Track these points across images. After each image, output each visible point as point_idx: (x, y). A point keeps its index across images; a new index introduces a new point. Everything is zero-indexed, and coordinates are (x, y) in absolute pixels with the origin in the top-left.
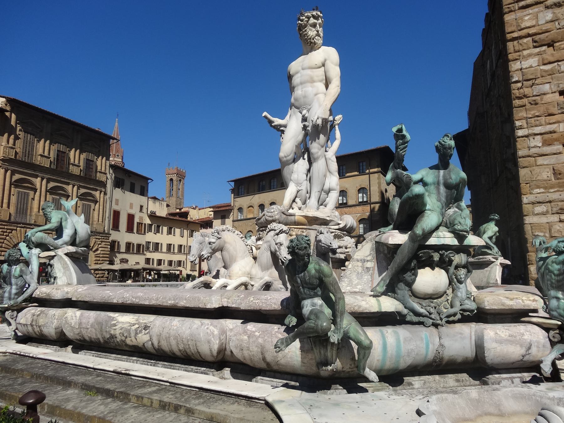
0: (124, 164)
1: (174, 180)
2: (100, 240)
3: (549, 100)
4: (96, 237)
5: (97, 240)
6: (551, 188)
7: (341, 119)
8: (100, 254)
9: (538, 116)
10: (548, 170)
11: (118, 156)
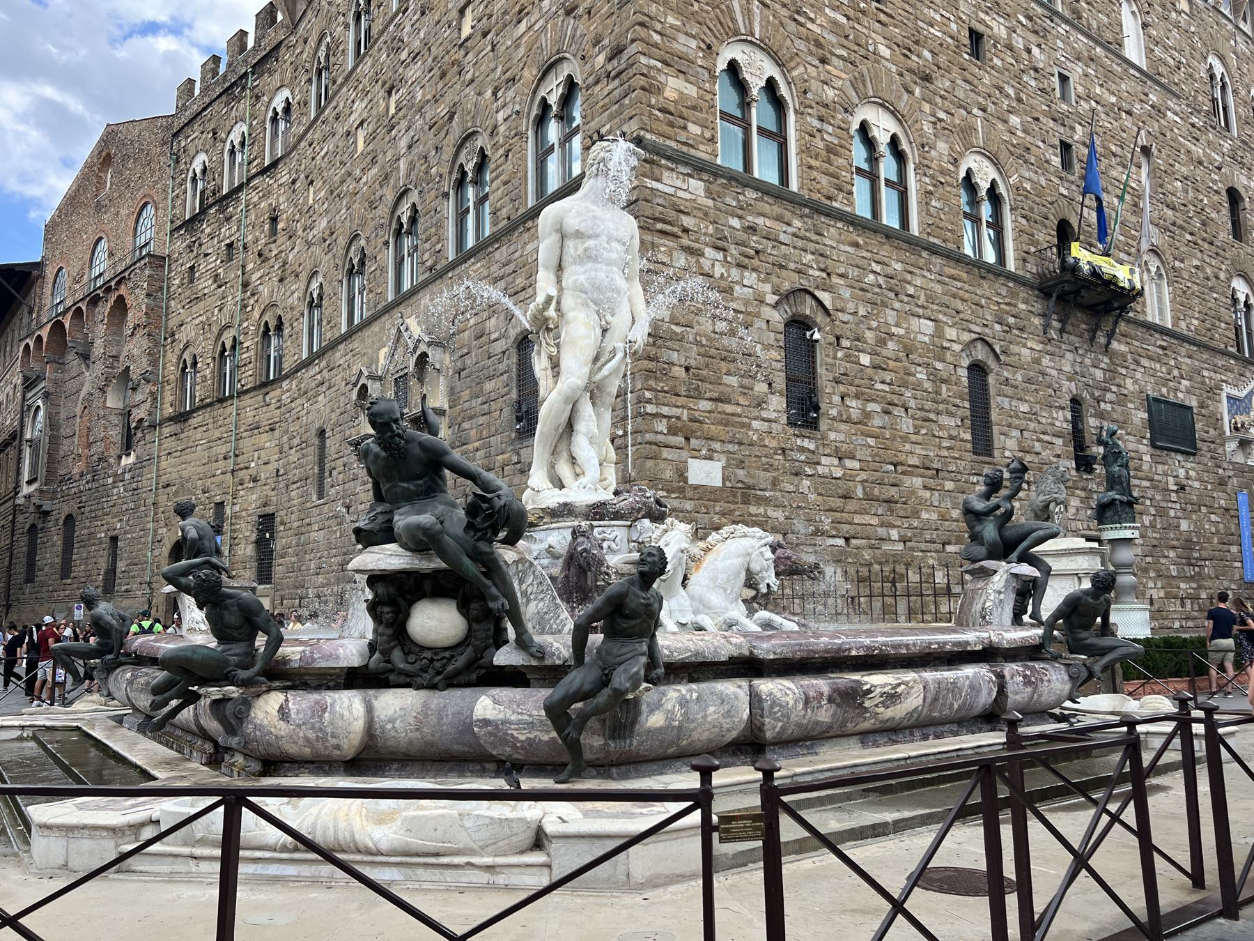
3: (677, 375)
6: (673, 492)
9: (666, 392)
10: (671, 467)
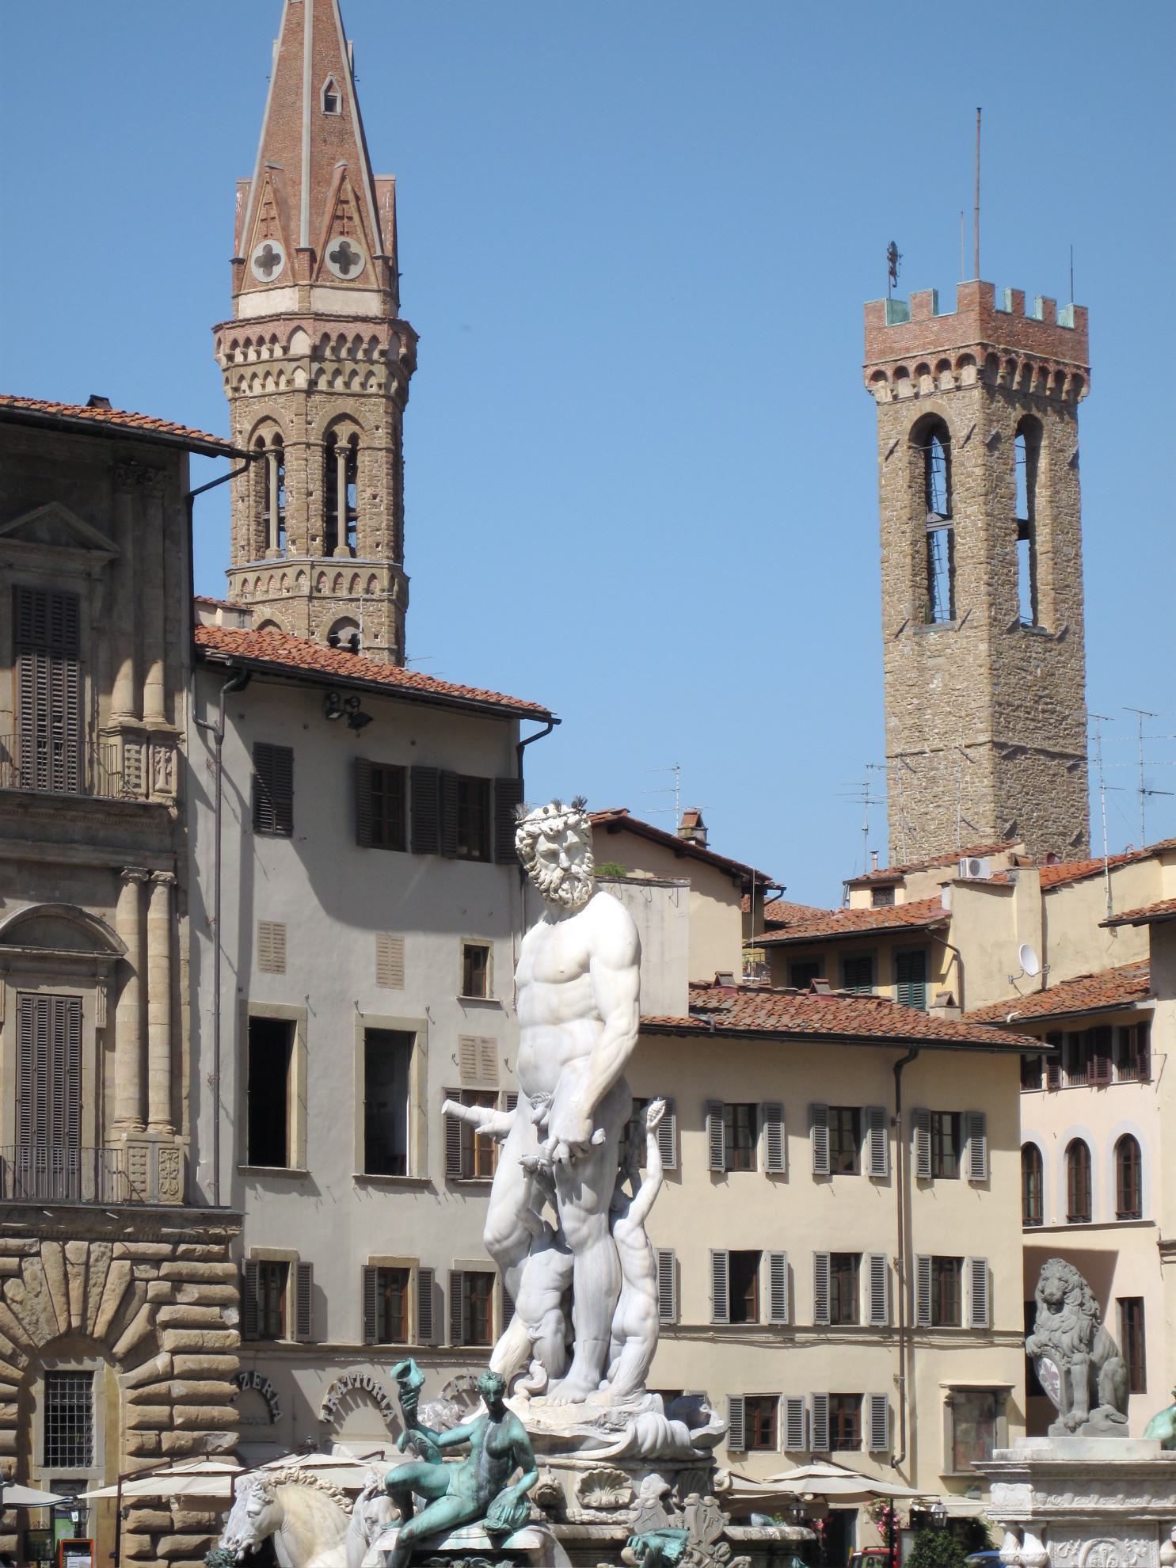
0: (413, 338)
1: (958, 429)
2: (166, 1268)
4: (134, 1247)
5: (143, 1271)
7: (661, 1115)
8: (169, 1375)
11: (344, 258)
